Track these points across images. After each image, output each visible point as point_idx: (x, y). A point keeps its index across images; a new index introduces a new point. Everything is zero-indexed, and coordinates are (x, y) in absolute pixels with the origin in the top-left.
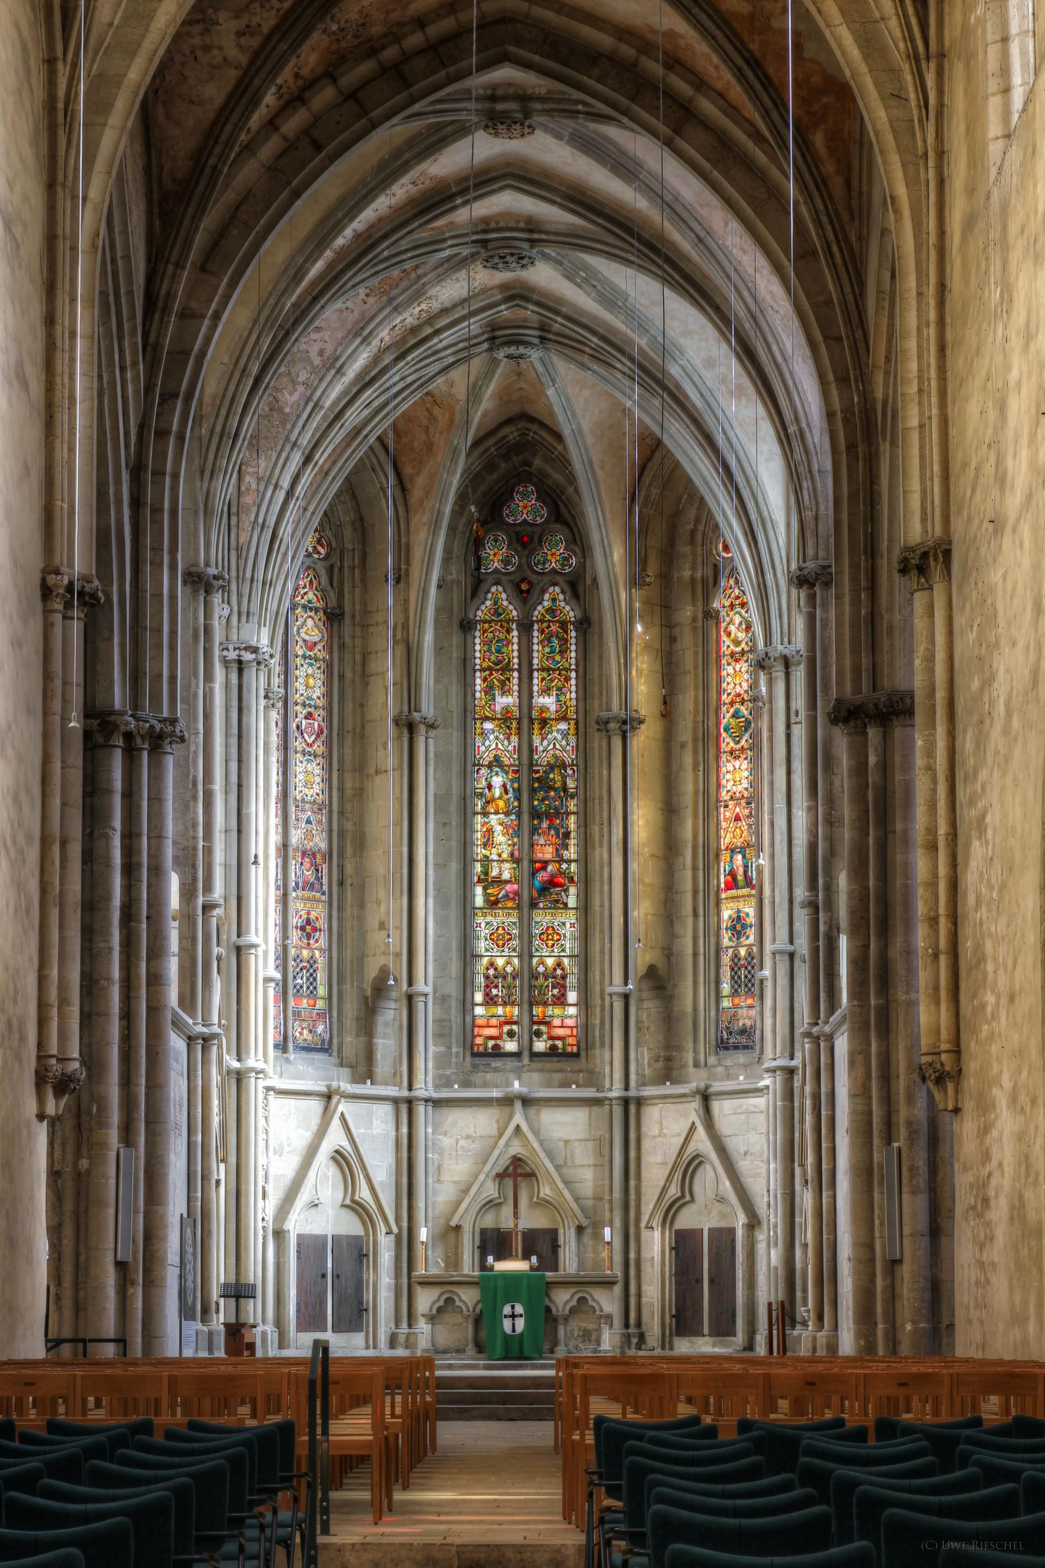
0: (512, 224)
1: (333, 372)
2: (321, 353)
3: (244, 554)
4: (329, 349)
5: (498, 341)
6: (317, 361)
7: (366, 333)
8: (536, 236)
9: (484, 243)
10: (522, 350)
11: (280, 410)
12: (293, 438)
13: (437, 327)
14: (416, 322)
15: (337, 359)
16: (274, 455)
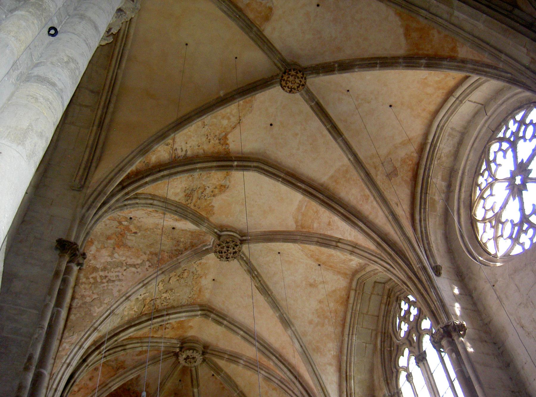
0: (233, 230)
1: (124, 298)
2: (119, 291)
3: (54, 377)
4: (124, 290)
5: (183, 350)
6: (116, 294)
7: (145, 282)
8: (244, 238)
9: (219, 237)
10: (195, 355)
11: (91, 315)
12: (96, 325)
13: (169, 312)
14: (160, 307)
15: (127, 293)
16: (83, 333)
